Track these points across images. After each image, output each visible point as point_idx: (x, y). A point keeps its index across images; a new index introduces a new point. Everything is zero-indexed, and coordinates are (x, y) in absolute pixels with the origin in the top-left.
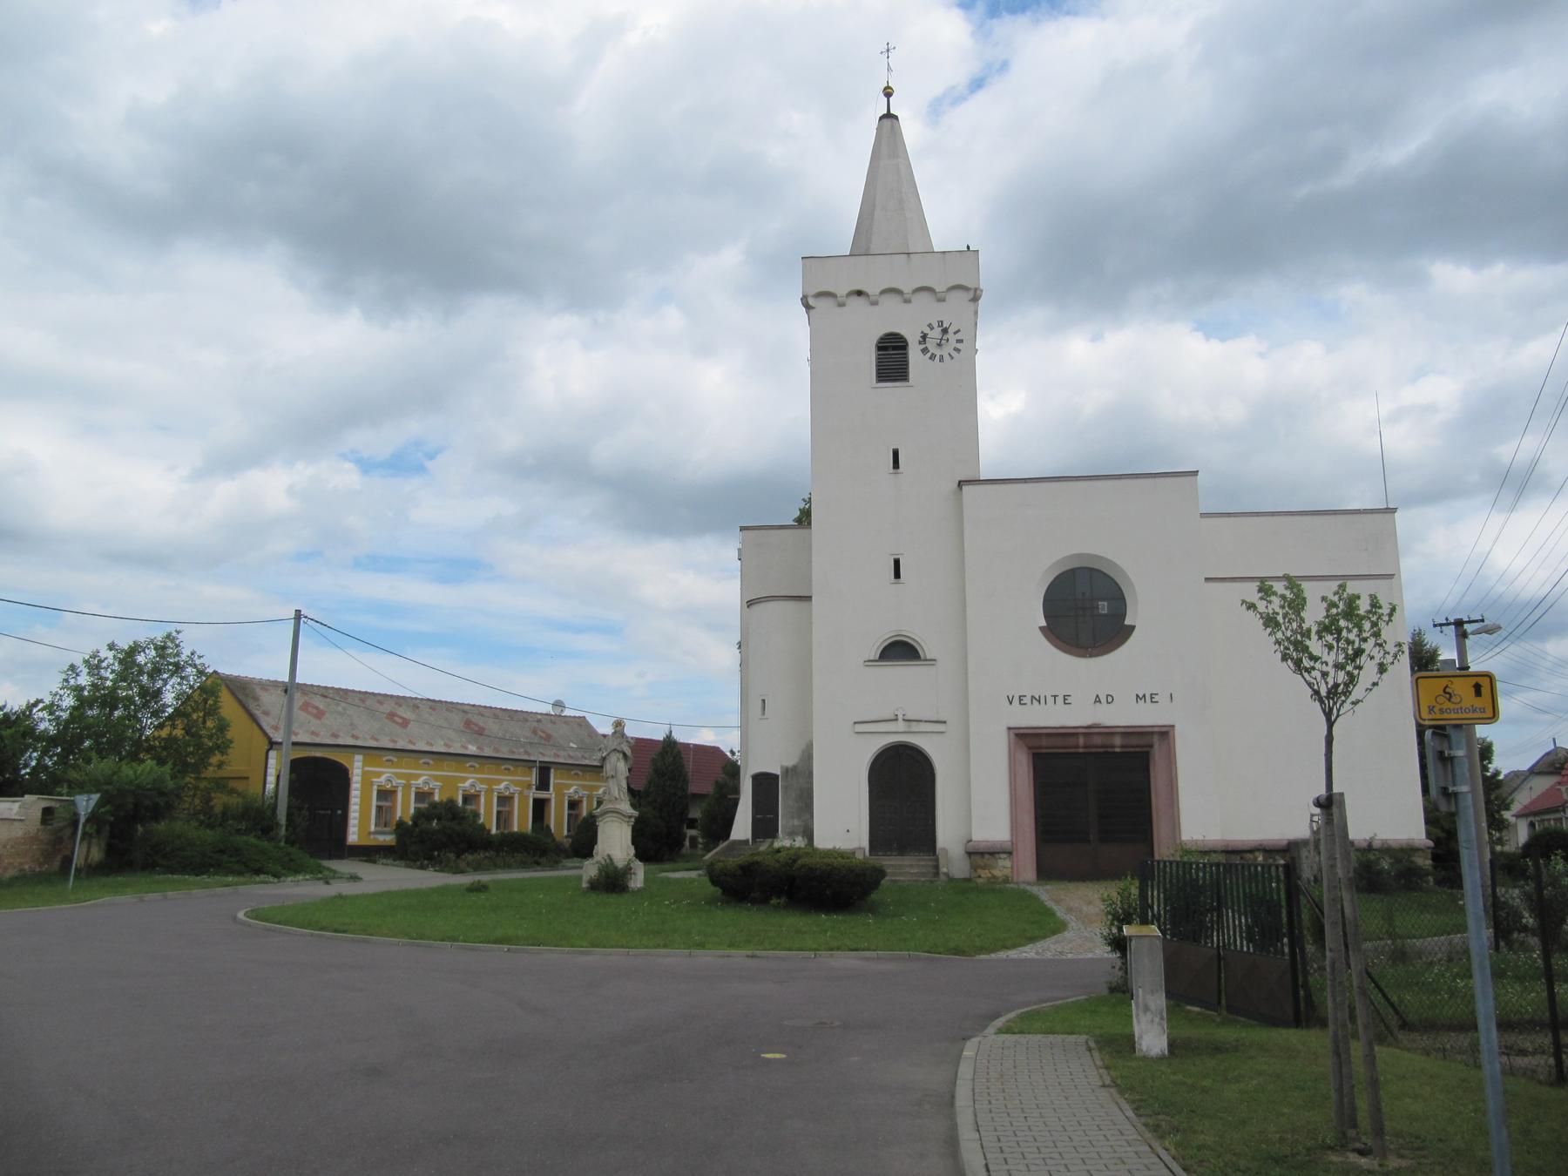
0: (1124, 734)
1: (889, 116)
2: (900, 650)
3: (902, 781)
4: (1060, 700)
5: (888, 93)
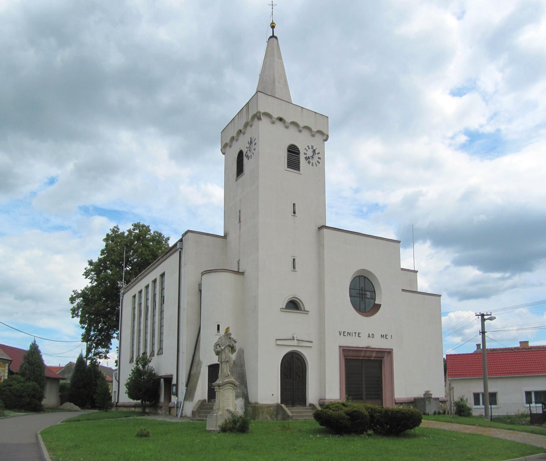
0: (378, 352)
1: (273, 36)
2: (294, 305)
3: (293, 370)
4: (357, 334)
5: (273, 27)
